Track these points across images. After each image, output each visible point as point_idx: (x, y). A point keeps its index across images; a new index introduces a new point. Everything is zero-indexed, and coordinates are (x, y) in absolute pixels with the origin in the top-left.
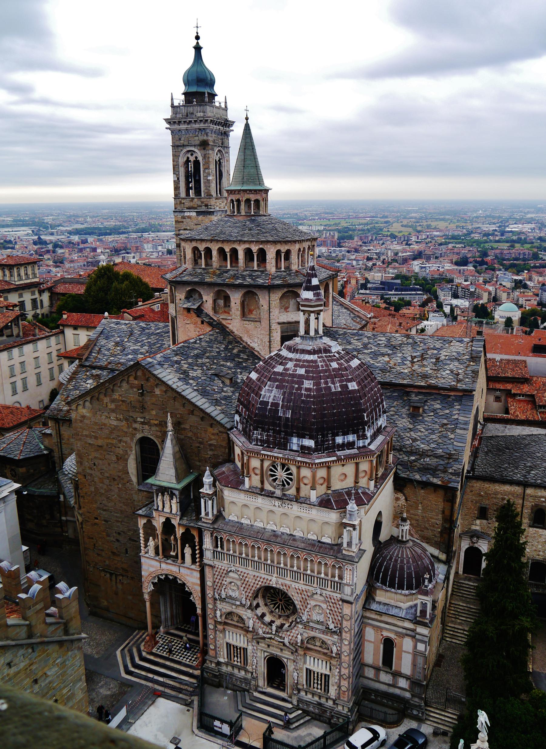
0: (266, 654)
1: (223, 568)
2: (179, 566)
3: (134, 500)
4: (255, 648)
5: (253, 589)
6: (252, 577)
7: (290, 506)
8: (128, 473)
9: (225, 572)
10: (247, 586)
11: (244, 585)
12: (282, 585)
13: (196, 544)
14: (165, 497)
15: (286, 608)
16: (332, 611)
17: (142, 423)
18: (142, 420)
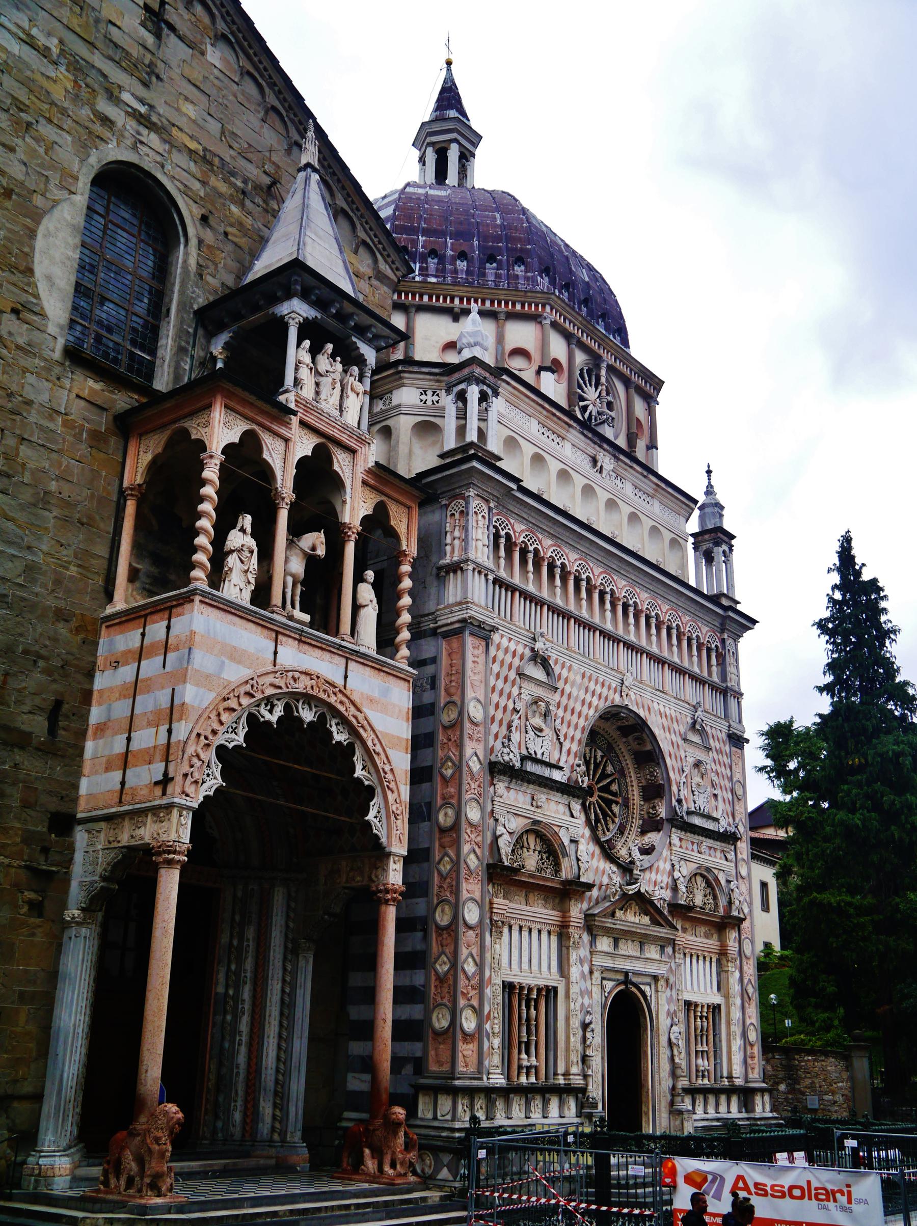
0: (609, 985)
1: (512, 646)
2: (347, 659)
3: (29, 403)
4: (586, 969)
5: (582, 722)
6: (579, 678)
7: (618, 482)
8: (29, 271)
9: (516, 662)
10: (568, 716)
11: (560, 713)
12: (637, 704)
13: (406, 568)
14: (324, 362)
15: (605, 815)
16: (718, 774)
17: (143, 120)
18: (143, 109)
